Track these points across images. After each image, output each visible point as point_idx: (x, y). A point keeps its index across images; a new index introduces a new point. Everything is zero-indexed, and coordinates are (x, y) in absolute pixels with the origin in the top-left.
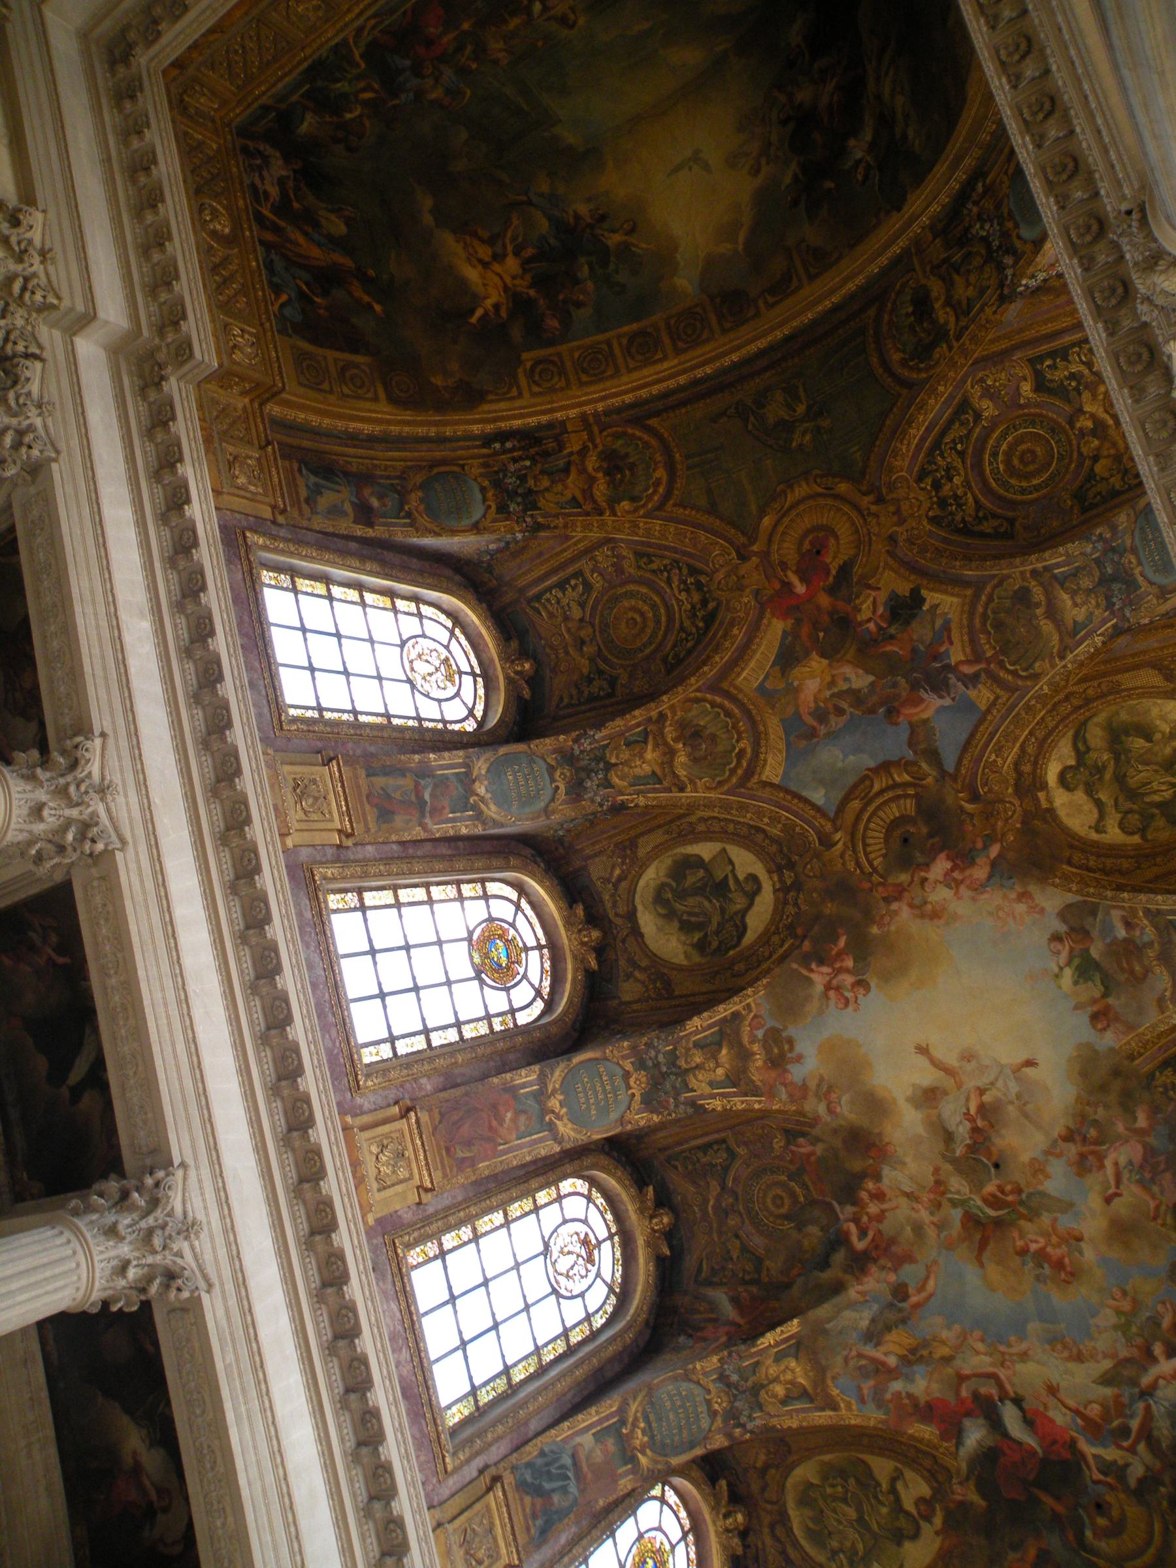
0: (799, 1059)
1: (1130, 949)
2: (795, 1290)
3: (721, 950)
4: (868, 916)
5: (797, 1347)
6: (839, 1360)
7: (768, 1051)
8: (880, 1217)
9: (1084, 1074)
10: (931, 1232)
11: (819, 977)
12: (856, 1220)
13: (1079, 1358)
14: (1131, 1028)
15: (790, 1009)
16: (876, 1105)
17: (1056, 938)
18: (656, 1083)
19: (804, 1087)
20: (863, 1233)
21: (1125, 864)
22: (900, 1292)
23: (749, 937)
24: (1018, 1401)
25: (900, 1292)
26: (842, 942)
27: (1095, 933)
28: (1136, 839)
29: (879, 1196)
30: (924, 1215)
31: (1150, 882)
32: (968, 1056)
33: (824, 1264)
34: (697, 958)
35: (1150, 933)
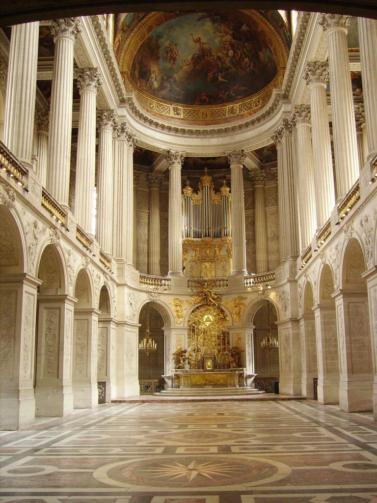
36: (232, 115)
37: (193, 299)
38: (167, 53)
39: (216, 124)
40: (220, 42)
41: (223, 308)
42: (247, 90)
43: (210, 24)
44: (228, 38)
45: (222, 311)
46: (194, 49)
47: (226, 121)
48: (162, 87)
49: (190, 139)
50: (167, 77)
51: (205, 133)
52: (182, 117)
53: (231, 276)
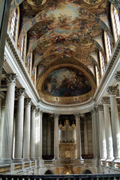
0: (47, 16)
1: (86, 13)
2: (43, 32)
3: (38, 4)
4: (58, 3)
5: (43, 37)
6: (46, 37)
7: (44, 15)
8: (52, 26)
9: (76, 19)
10: (57, 27)
11: (51, 8)
12: (49, 26)
13: (68, 34)
14: (82, 17)
15: (47, 11)
16: (54, 18)
17: (78, 9)
18: (33, 23)
19: (47, 18)
20: (50, 27)
21: (88, 6)
22: (53, 31)
23: (42, 4)
24: (61, 36)
25: (53, 31)
26: (54, 5)
27: (83, 11)
28: (90, 4)
29: (53, 24)
30: (57, 26)
31: (91, 9)
32: (65, 15)
33: (46, 29)
34: (35, 5)
35: (88, 13)
36: (76, 101)
37: (63, 167)
38: (54, 80)
39: (71, 104)
40: (72, 76)
41: (73, 171)
42: (81, 93)
43: (68, 71)
44: (74, 75)
45: (73, 172)
46: (63, 78)
47: (74, 103)
48: (52, 91)
49: (61, 109)
50: (54, 88)
51: (66, 107)
52: (59, 101)
53: (76, 159)
